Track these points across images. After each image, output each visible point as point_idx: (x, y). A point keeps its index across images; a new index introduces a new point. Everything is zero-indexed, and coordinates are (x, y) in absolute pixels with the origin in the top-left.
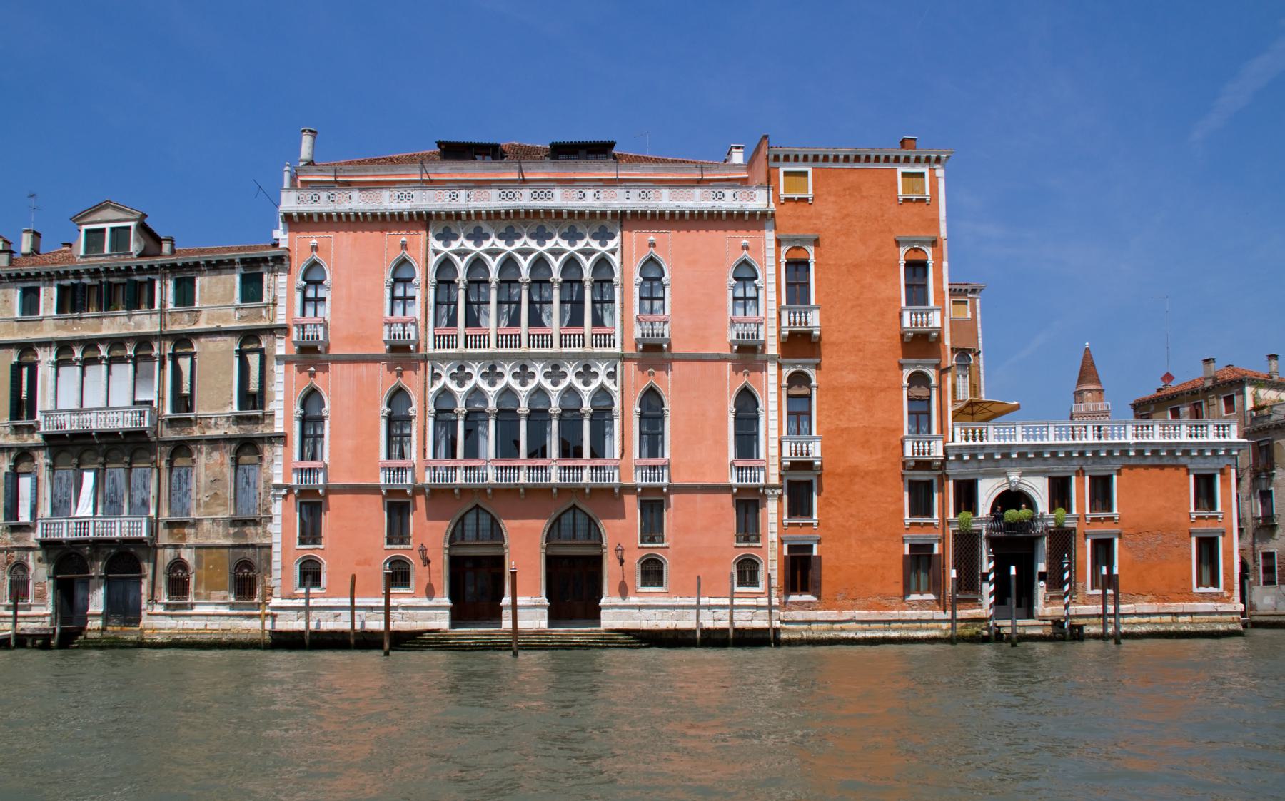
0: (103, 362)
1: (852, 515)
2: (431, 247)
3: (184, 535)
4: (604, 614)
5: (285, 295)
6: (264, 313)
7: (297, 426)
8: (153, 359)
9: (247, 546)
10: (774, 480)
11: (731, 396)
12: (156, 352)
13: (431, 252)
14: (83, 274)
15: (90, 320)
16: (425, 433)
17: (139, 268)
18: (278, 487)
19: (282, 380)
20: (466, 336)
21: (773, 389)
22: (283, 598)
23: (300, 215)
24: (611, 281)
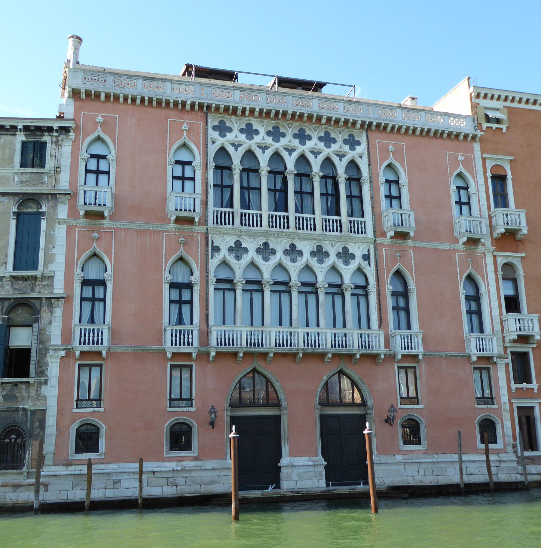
6: (46, 179)
9: (17, 410)
11: (461, 280)
18: (56, 349)
21: (491, 275)
22: (55, 465)
23: (88, 94)
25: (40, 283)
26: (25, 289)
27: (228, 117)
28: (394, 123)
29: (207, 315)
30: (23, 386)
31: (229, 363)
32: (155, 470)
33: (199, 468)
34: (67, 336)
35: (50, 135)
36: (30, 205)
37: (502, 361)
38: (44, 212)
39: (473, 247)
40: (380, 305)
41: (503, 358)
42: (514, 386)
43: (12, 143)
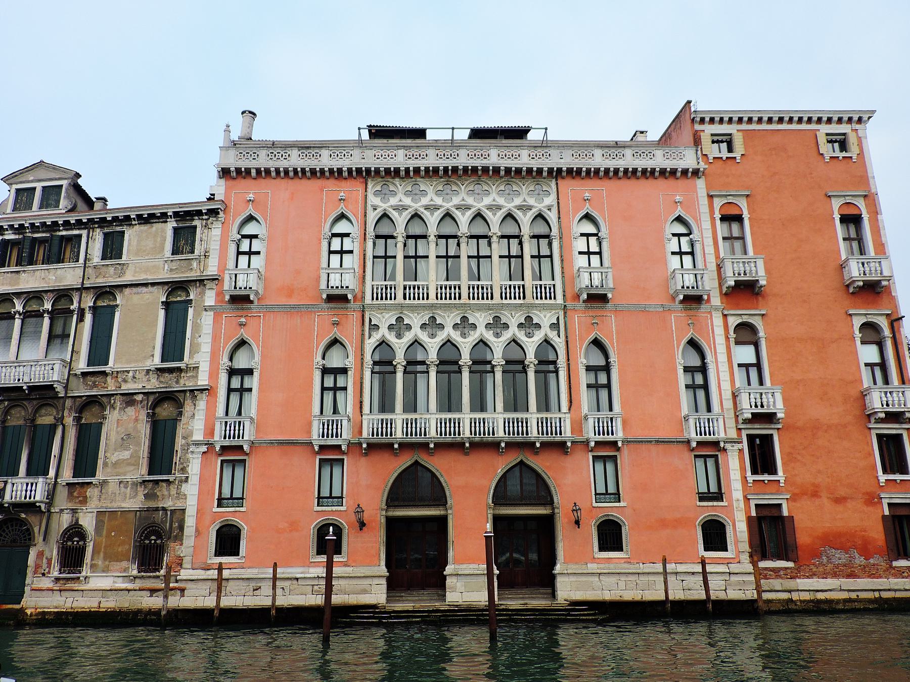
0: (17, 316)
1: (819, 472)
2: (369, 203)
4: (560, 582)
5: (218, 247)
6: (195, 264)
7: (223, 377)
8: (72, 312)
9: (157, 509)
10: (733, 434)
12: (74, 307)
13: (369, 209)
14: (7, 230)
15: (9, 275)
16: (362, 383)
17: (67, 224)
18: (197, 444)
19: (210, 331)
21: (720, 340)
23: (238, 171)
25: (185, 375)
26: (170, 382)
27: (391, 180)
28: (590, 167)
29: (361, 402)
30: (164, 484)
31: (386, 456)
32: (298, 576)
33: (347, 575)
34: (210, 432)
35: (199, 219)
36: (179, 293)
37: (733, 446)
38: (191, 300)
39: (694, 306)
40: (570, 383)
41: (735, 442)
42: (751, 478)
43: (163, 231)
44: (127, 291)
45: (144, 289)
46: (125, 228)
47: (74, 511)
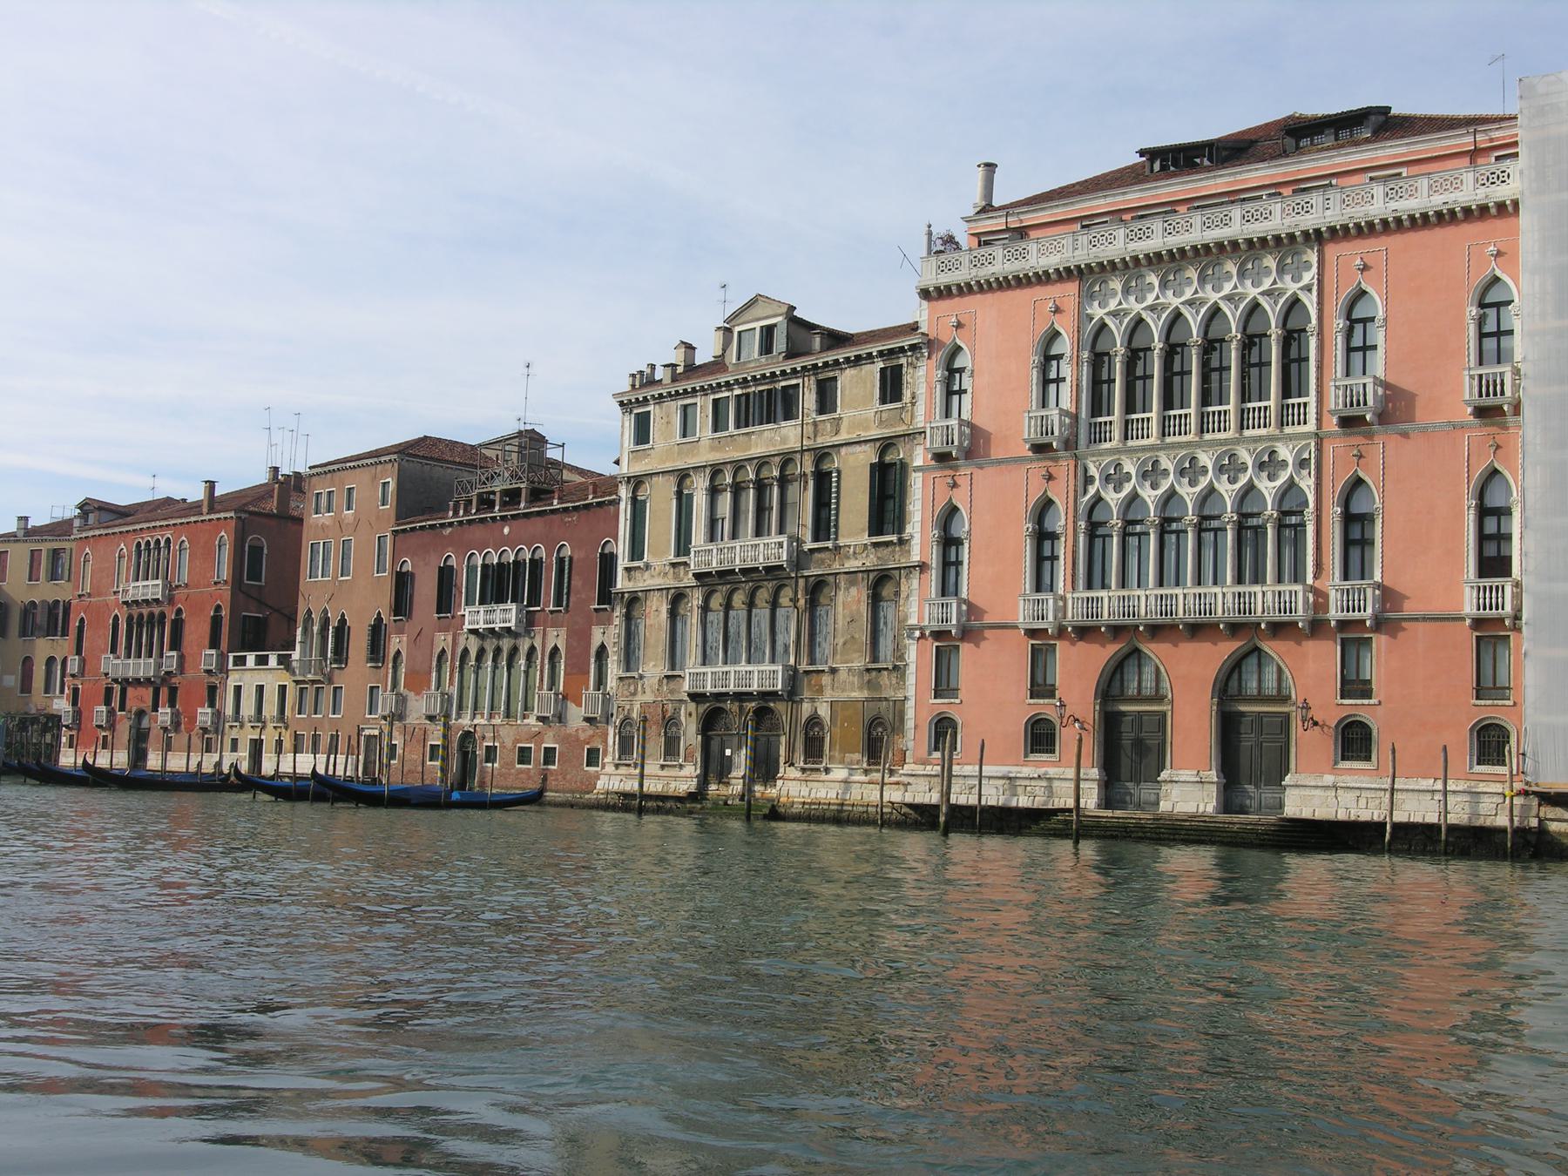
3: (821, 686)
9: (880, 700)
14: (734, 384)
17: (783, 373)
18: (912, 629)
20: (1127, 422)
24: (1304, 330)
30: (886, 673)
44: (843, 450)
45: (858, 448)
46: (837, 373)
47: (812, 700)
